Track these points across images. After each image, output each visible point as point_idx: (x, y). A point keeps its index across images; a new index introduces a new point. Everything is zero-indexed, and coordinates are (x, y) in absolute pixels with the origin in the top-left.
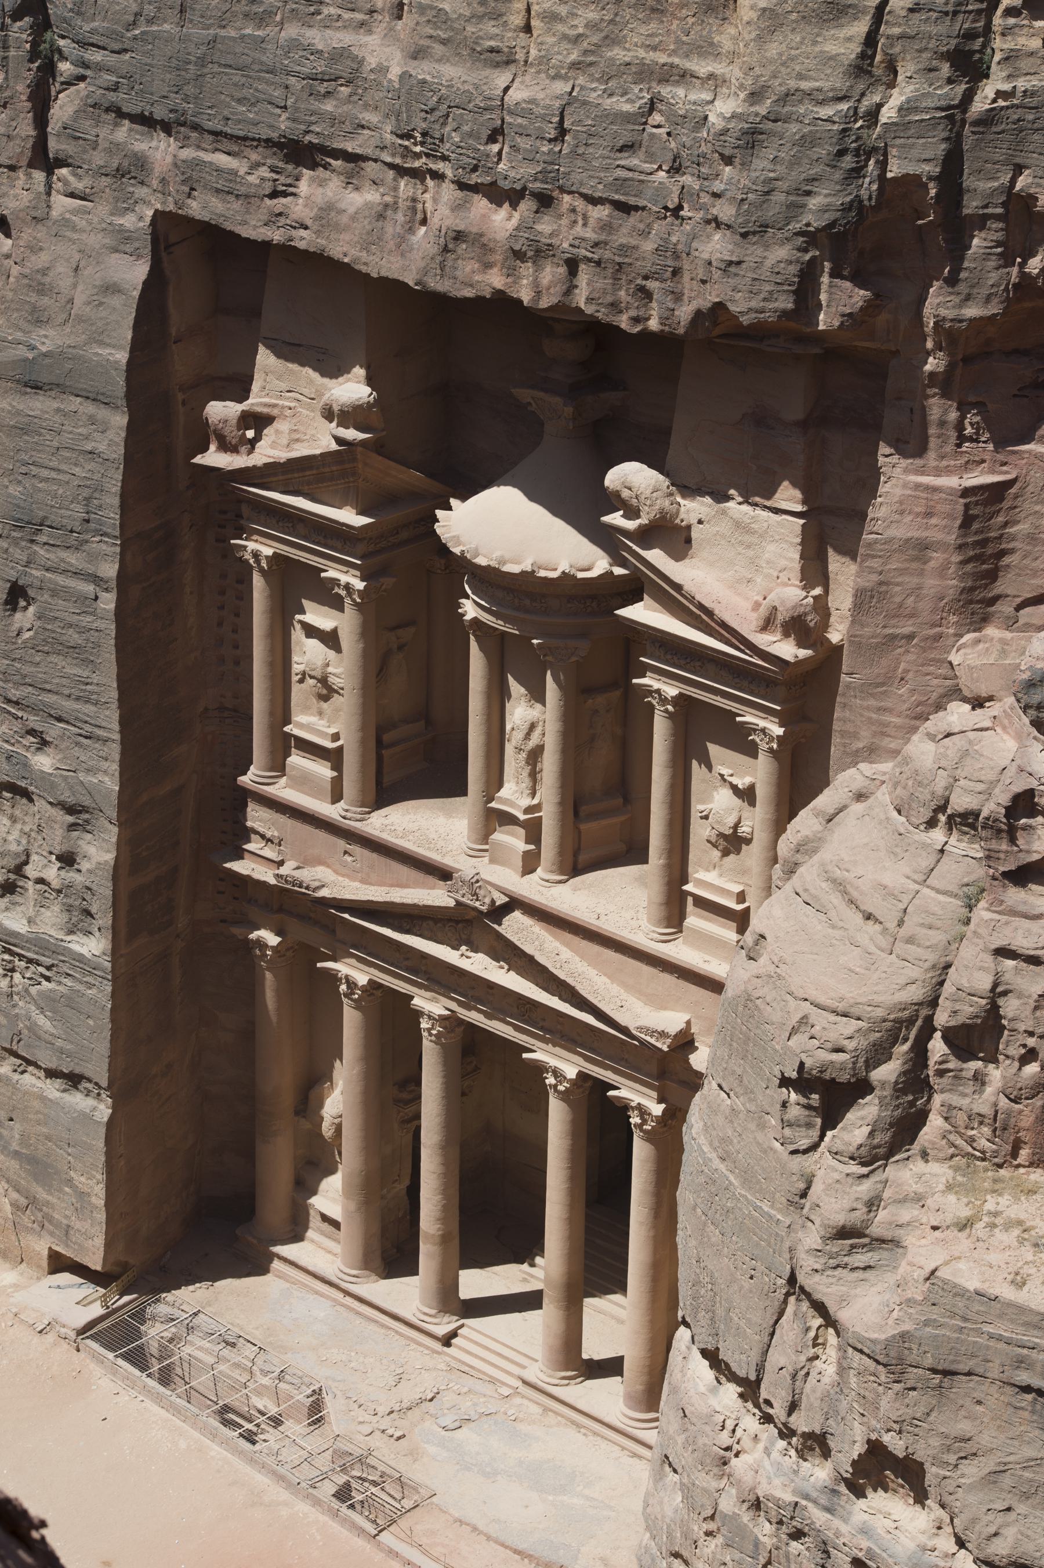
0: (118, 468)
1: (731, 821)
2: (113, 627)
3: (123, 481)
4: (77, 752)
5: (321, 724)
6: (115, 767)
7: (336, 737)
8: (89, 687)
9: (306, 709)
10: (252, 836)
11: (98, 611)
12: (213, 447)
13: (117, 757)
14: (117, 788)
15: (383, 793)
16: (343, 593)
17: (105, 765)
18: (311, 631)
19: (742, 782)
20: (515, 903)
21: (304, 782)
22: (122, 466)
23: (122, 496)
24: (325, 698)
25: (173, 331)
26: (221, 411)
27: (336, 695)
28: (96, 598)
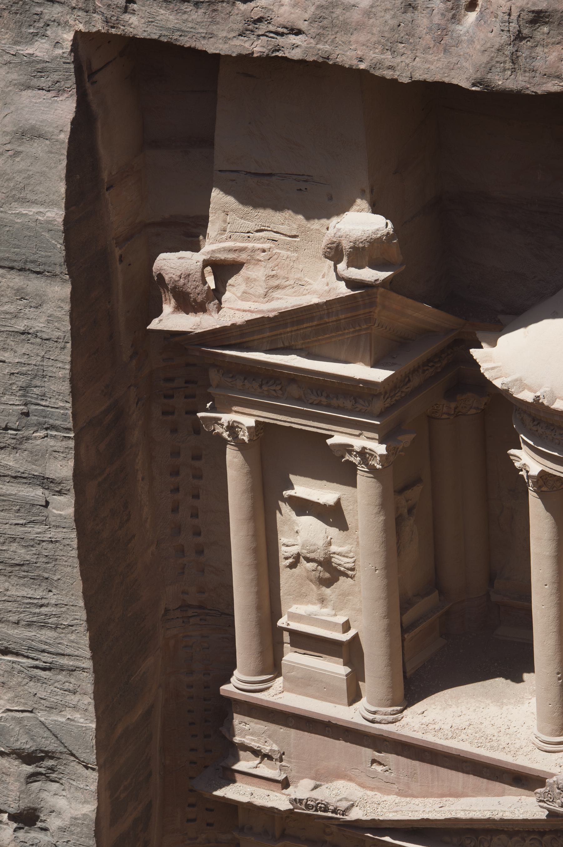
0: (63, 348)
2: (74, 535)
3: (72, 362)
4: (33, 687)
6: (88, 701)
7: (346, 627)
8: (44, 610)
9: (301, 597)
10: (242, 753)
11: (51, 519)
12: (168, 308)
13: (90, 688)
14: (94, 726)
16: (356, 460)
17: (73, 699)
18: (303, 507)
21: (307, 682)
22: (69, 345)
23: (72, 380)
24: (328, 583)
25: (105, 176)
27: (342, 579)
28: (47, 504)
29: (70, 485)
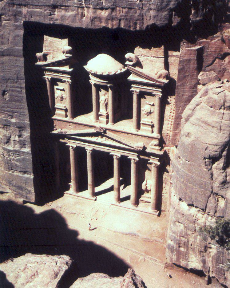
1: (149, 110)
5: (62, 105)
15: (74, 115)
19: (152, 103)
20: (106, 129)
26: (39, 55)
29: (25, 88)
